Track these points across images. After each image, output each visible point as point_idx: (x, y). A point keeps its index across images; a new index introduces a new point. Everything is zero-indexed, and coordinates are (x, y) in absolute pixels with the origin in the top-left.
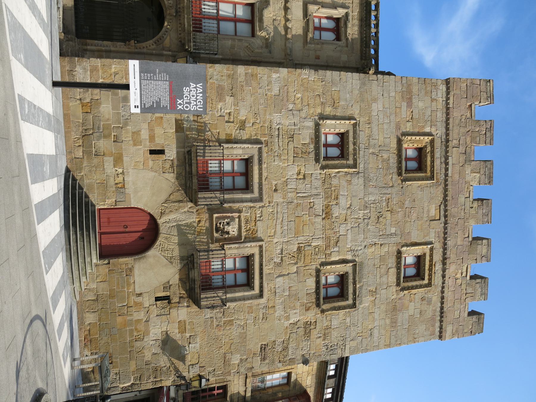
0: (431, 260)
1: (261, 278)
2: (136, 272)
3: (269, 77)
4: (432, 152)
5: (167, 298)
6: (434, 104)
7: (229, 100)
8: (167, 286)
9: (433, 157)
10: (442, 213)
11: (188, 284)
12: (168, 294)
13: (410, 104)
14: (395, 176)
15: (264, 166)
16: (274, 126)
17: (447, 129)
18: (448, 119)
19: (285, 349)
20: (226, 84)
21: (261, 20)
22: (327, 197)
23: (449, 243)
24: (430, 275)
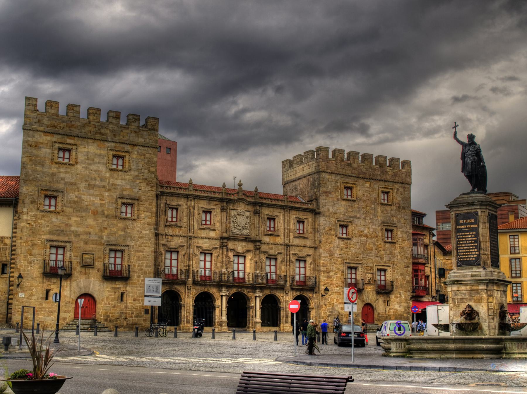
0: (384, 188)
2: (380, 312)
3: (323, 257)
7: (331, 274)
8: (384, 302)
9: (348, 183)
10: (368, 180)
13: (330, 193)
15: (351, 262)
16: (338, 256)
19: (407, 258)
21: (301, 257)
22: (361, 235)
23: (379, 178)
24: (389, 189)
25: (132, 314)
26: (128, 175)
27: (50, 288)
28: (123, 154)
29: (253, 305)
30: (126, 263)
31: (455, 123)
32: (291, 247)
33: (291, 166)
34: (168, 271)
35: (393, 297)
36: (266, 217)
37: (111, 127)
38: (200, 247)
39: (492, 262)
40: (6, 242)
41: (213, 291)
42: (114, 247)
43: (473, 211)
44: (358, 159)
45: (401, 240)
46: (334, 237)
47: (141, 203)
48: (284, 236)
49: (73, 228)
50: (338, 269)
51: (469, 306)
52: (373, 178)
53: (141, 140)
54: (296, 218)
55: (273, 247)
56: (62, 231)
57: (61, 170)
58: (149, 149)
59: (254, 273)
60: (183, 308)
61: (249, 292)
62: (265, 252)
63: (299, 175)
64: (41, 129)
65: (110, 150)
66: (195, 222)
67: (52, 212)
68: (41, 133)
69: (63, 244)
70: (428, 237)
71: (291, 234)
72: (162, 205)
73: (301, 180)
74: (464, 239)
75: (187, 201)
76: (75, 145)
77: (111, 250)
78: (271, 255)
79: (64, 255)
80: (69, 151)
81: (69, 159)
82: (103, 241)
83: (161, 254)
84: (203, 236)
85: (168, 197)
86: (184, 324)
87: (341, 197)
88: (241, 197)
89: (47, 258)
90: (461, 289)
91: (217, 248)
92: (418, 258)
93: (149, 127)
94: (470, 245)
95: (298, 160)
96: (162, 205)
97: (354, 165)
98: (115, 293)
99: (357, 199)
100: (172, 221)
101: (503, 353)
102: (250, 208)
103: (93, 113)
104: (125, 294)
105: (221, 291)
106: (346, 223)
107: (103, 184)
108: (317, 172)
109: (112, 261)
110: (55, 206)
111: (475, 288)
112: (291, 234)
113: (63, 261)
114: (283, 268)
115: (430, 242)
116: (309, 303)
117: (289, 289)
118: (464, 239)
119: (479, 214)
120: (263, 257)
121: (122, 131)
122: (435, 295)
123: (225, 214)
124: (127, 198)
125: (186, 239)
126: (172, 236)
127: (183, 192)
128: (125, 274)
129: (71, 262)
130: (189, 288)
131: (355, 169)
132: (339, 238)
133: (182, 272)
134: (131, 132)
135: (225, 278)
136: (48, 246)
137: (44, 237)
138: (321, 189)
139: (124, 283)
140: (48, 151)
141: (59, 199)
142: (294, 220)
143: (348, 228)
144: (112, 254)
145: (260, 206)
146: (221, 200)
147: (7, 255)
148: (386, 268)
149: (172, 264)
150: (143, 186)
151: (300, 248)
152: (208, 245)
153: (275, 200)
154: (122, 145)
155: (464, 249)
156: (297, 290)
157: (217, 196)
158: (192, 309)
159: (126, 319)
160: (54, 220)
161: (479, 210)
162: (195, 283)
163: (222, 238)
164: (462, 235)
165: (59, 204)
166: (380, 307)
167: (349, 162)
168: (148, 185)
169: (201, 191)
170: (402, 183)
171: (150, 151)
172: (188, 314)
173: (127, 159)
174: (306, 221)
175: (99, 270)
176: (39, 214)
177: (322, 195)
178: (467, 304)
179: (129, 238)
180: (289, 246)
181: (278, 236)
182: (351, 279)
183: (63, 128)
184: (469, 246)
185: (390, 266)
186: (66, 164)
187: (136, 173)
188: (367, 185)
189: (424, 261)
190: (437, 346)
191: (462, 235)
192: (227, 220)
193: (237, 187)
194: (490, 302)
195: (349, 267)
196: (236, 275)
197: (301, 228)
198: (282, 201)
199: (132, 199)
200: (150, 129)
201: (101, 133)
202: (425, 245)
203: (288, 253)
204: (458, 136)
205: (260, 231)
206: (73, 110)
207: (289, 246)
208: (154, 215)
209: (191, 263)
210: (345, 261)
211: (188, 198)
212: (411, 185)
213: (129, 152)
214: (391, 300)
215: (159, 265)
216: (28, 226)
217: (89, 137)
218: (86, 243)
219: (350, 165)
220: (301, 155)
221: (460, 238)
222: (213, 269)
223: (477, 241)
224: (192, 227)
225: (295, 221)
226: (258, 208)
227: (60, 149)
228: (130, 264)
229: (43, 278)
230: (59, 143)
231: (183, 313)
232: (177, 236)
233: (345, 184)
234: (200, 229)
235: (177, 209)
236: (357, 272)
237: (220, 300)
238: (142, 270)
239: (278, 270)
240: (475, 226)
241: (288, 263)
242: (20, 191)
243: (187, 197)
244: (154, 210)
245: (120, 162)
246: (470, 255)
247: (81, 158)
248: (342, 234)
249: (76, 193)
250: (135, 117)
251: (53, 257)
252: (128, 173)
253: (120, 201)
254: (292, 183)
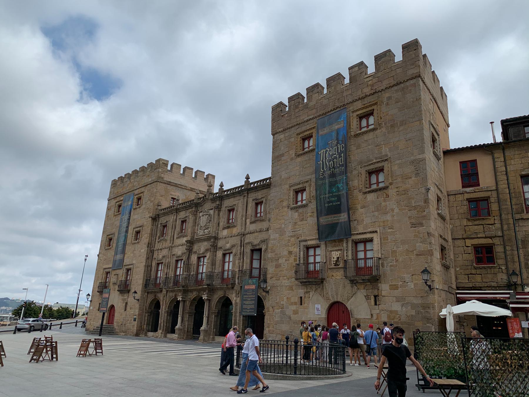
0: (360, 109)
1: (365, 233)
2: (359, 317)
5: (375, 297)
7: (280, 261)
8: (367, 297)
11: (367, 283)
12: (372, 297)
13: (283, 155)
17: (292, 127)
18: (288, 128)
19: (415, 208)
21: (256, 246)
23: (350, 100)
24: (371, 106)
35: (384, 288)
38: (174, 255)
45: (399, 180)
46: (286, 209)
50: (290, 253)
54: (253, 200)
106: (301, 186)
126: (161, 249)
132: (292, 209)
148: (368, 236)
151: (256, 234)
166: (359, 307)
170: (397, 84)
181: (235, 226)
185: (376, 232)
214: (384, 293)
233: (301, 135)
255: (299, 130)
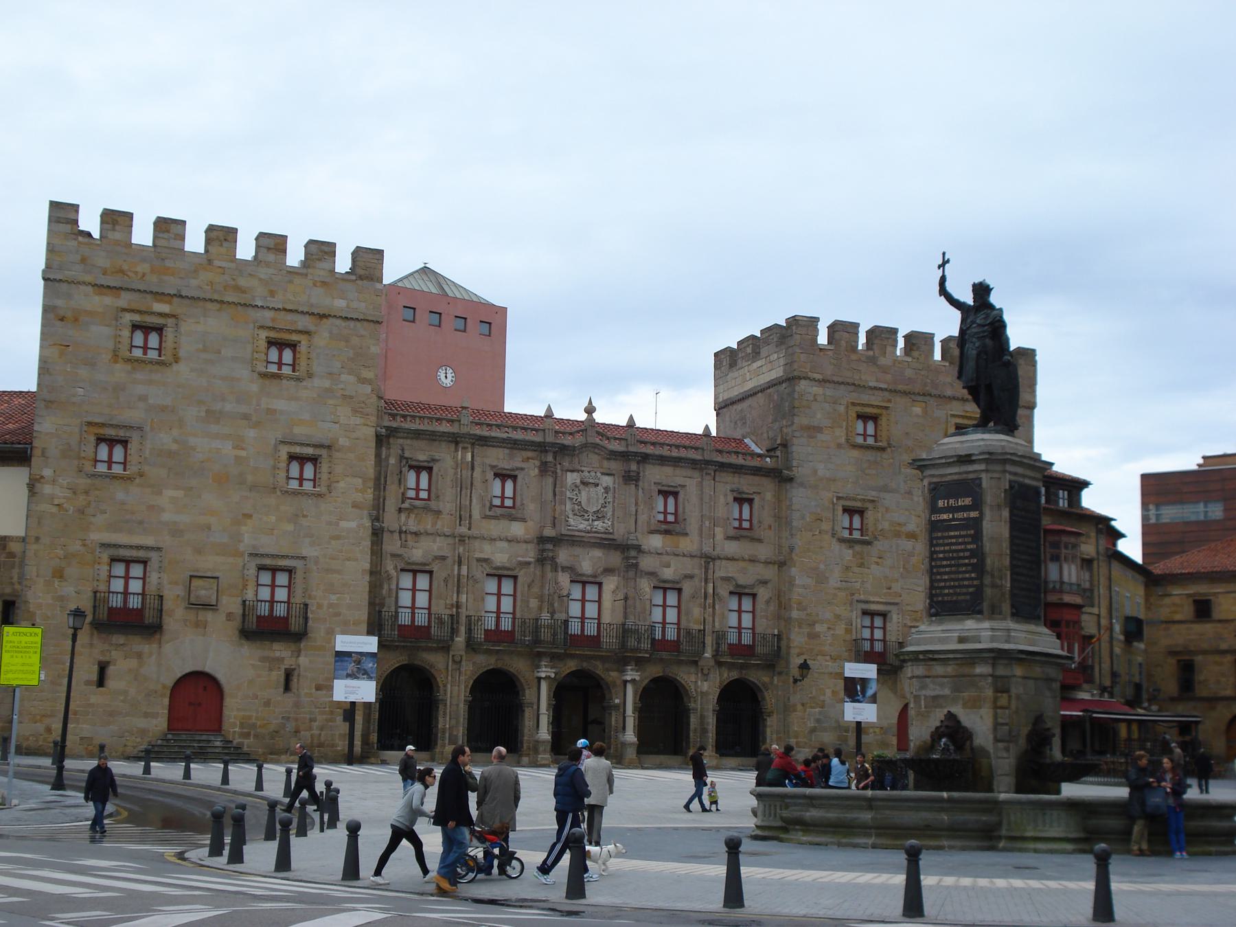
4: (863, 405)
6: (819, 398)
7: (819, 628)
10: (920, 398)
13: (819, 429)
14: (885, 455)
15: (872, 599)
16: (839, 585)
18: (834, 382)
20: (806, 630)
21: (745, 587)
22: (898, 535)
25: (311, 720)
26: (306, 388)
27: (107, 659)
28: (294, 337)
29: (617, 701)
30: (298, 599)
31: (944, 254)
32: (718, 563)
33: (733, 365)
34: (405, 618)
36: (655, 489)
37: (263, 273)
38: (486, 560)
39: (1013, 606)
40: (13, 550)
41: (518, 666)
42: (268, 562)
43: (971, 476)
44: (896, 346)
46: (827, 537)
47: (337, 455)
48: (701, 535)
49: (166, 517)
50: (838, 617)
51: (951, 716)
52: (934, 392)
53: (340, 304)
54: (732, 491)
55: (674, 561)
56: (141, 523)
57: (139, 376)
58: (359, 324)
59: (624, 625)
60: (441, 707)
61: (608, 670)
62: (652, 574)
63: (749, 386)
64: (89, 278)
65: (261, 327)
66: (474, 501)
67: (115, 477)
68: (90, 289)
69: (141, 554)
70: (1093, 540)
71: (718, 530)
72: (392, 461)
73: (755, 398)
74: (947, 548)
75: (457, 450)
76: (174, 316)
77: (261, 568)
78: (665, 581)
79: (144, 579)
80: (159, 330)
81: (160, 350)
82: (242, 547)
83: (389, 578)
84: (495, 534)
85: (409, 442)
86: (444, 746)
87: (847, 440)
88: (590, 440)
89: (102, 587)
90: (934, 673)
91: (529, 563)
92: (1061, 591)
93: (361, 272)
94: (962, 561)
95: (749, 350)
96: (392, 461)
97: (882, 361)
98: (271, 670)
99: (890, 445)
100: (417, 498)
101: (1000, 838)
102: (615, 466)
103: (218, 238)
104: (296, 673)
105: (538, 667)
106: (859, 504)
107: (244, 409)
108: (789, 379)
109: (265, 593)
110: (124, 464)
111: (966, 670)
112: (718, 530)
113: (143, 594)
114: (697, 612)
115: (1098, 553)
116: (764, 699)
117: (712, 663)
118: (947, 548)
119: (984, 484)
120: (645, 585)
121: (291, 282)
122: (1107, 683)
123: (550, 480)
124: (302, 444)
125: (450, 540)
126: (416, 534)
127: (445, 427)
128: (295, 626)
129: (161, 597)
130: (457, 659)
131: (885, 370)
132: (842, 540)
133: (440, 621)
134: (315, 285)
135: (545, 635)
136: (105, 557)
137: (96, 536)
138: (796, 420)
139: (293, 646)
140: (106, 331)
141: (133, 447)
142: (726, 495)
143: (866, 515)
144: (265, 578)
145: (638, 463)
146: (541, 447)
147: (15, 579)
149: (414, 600)
150: (344, 413)
151: (741, 564)
152: (507, 556)
153: (678, 447)
154: (290, 317)
155: (946, 573)
156: (731, 666)
157: (531, 436)
158: (462, 709)
159: (297, 731)
160: (120, 495)
161: (983, 476)
162: (471, 645)
163: (542, 540)
164: (943, 538)
165: (133, 459)
167: (871, 353)
168: (355, 411)
169: (490, 425)
171: (361, 328)
172: (453, 722)
173: (303, 348)
174: (757, 498)
175: (230, 616)
176: (83, 482)
177: (797, 434)
178: (945, 711)
179: (307, 540)
180: (714, 559)
181: (686, 534)
182: (872, 640)
183: (144, 275)
184: (959, 565)
186: (151, 363)
187: (327, 384)
188: (917, 410)
189: (1078, 600)
190: (832, 815)
191: (943, 538)
192: (555, 495)
193: (582, 416)
194: (1002, 708)
195: (865, 613)
196: (575, 628)
197: (746, 515)
198: (696, 449)
199: (315, 446)
200: (361, 278)
201: (238, 289)
202: (1083, 560)
203: (710, 576)
204: (949, 287)
205: (639, 522)
206: (168, 231)
207: (714, 559)
208: (371, 484)
209: (463, 598)
210: (856, 597)
211: (457, 443)
212: (1036, 411)
213: (307, 333)
215: (383, 605)
216: (54, 510)
217: (208, 296)
218: (198, 551)
219: (872, 360)
220: (753, 337)
221: (937, 545)
222: (518, 615)
223: (979, 554)
224: (465, 514)
225: (730, 498)
226: (634, 467)
227: (135, 327)
228: (308, 601)
229: (92, 635)
230: (132, 311)
231: (441, 719)
232: (428, 534)
233: (859, 409)
234: (486, 517)
235: (430, 470)
236: (888, 625)
237: (535, 689)
238: (338, 614)
239: (683, 618)
240: (973, 514)
241: (710, 601)
242: (36, 427)
243: (455, 440)
244: (371, 472)
245: (288, 356)
246: (959, 586)
247: (187, 347)
248: (851, 529)
249: (175, 432)
250: (326, 249)
251: (118, 585)
252: (304, 383)
253: (284, 451)
254: (735, 407)
255: (854, 397)
